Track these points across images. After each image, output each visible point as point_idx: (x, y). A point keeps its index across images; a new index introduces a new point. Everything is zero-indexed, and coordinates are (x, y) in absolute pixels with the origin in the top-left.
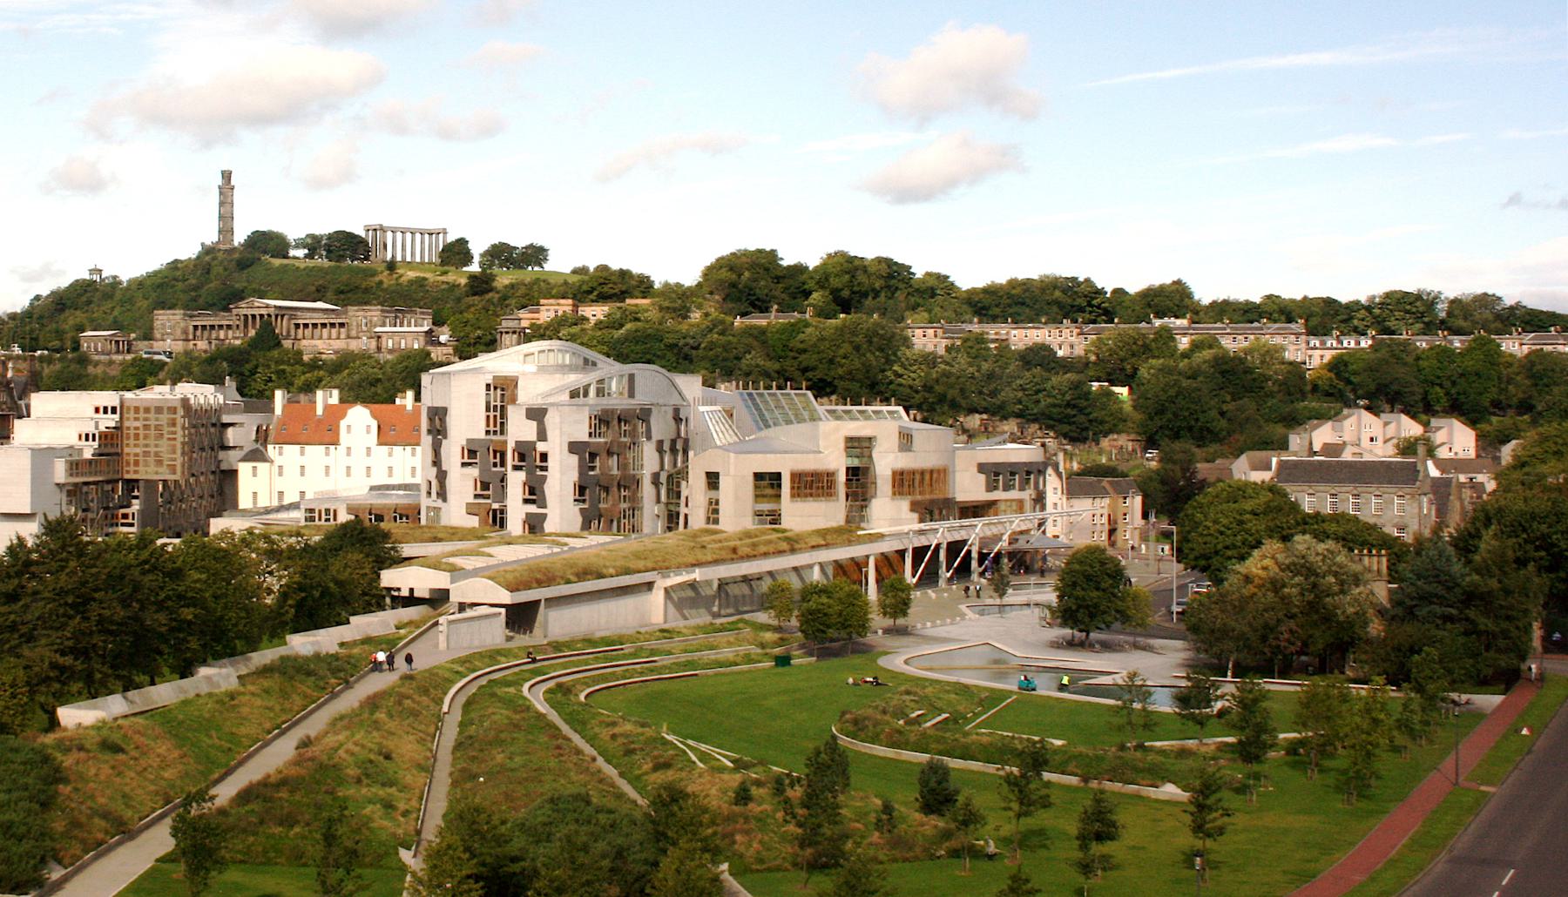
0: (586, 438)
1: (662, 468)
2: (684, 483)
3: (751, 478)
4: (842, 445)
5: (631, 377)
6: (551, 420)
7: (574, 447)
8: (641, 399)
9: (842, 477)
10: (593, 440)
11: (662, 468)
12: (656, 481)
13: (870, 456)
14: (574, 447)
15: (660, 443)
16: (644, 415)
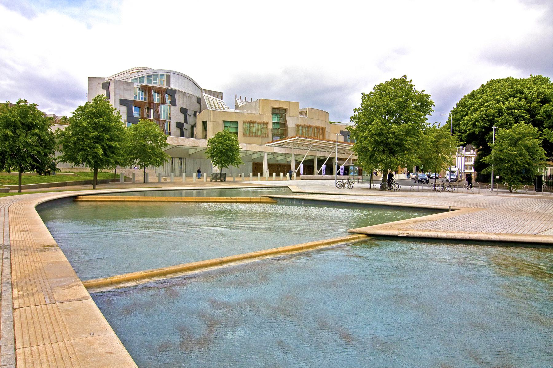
0: (133, 99)
1: (186, 121)
2: (195, 128)
3: (222, 123)
4: (270, 111)
5: (168, 77)
6: (112, 88)
7: (123, 102)
8: (173, 86)
9: (271, 126)
10: (137, 100)
11: (186, 121)
12: (180, 126)
13: (285, 118)
14: (123, 102)
15: (184, 111)
16: (172, 93)
